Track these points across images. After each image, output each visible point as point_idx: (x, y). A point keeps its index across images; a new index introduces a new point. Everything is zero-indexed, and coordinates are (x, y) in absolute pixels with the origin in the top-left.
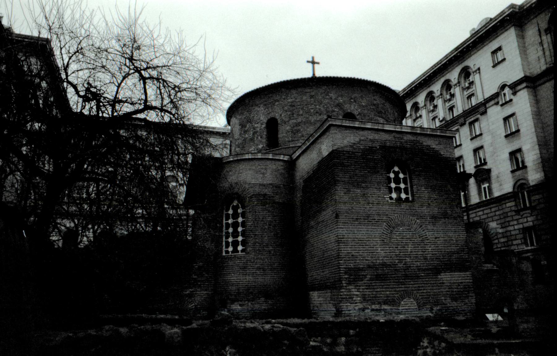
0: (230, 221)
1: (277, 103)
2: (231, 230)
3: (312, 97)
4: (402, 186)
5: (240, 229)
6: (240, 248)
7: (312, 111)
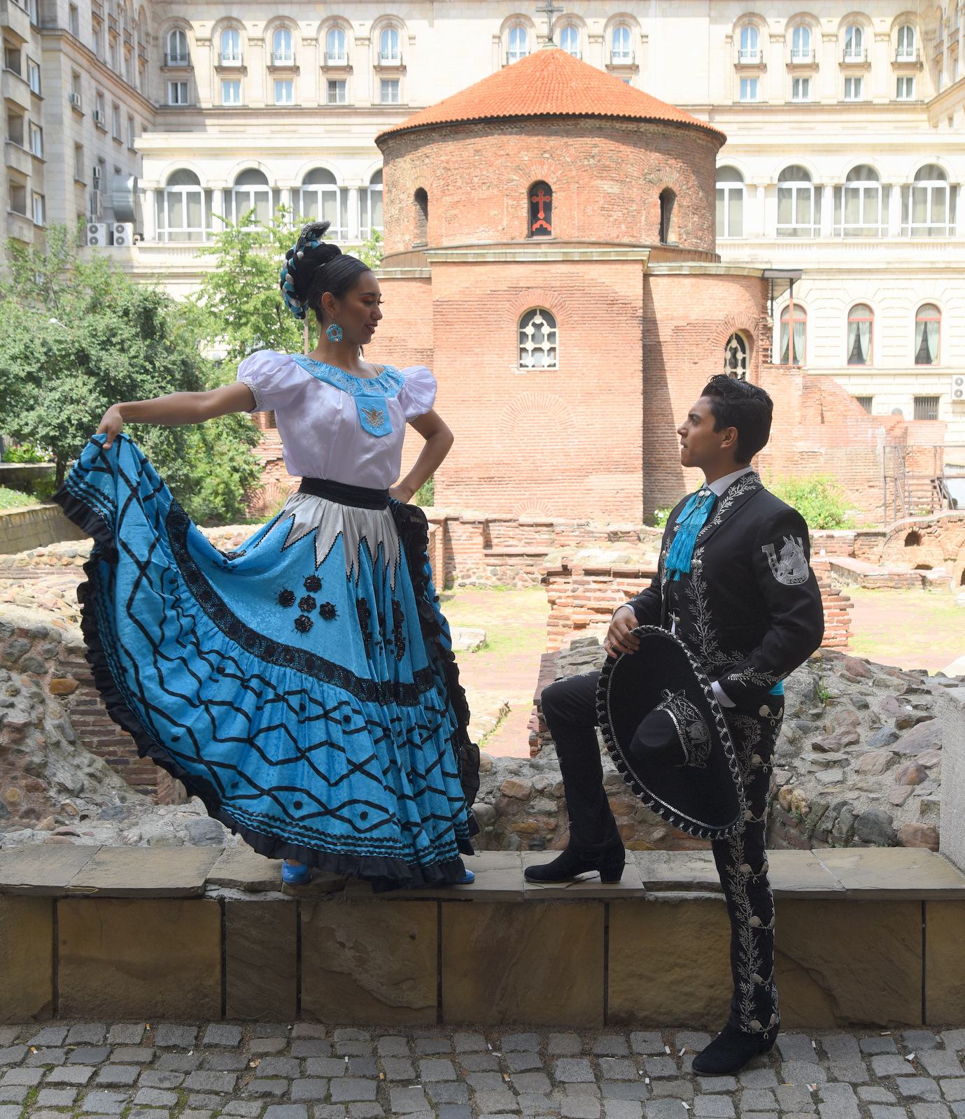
1: (427, 161)
7: (476, 180)
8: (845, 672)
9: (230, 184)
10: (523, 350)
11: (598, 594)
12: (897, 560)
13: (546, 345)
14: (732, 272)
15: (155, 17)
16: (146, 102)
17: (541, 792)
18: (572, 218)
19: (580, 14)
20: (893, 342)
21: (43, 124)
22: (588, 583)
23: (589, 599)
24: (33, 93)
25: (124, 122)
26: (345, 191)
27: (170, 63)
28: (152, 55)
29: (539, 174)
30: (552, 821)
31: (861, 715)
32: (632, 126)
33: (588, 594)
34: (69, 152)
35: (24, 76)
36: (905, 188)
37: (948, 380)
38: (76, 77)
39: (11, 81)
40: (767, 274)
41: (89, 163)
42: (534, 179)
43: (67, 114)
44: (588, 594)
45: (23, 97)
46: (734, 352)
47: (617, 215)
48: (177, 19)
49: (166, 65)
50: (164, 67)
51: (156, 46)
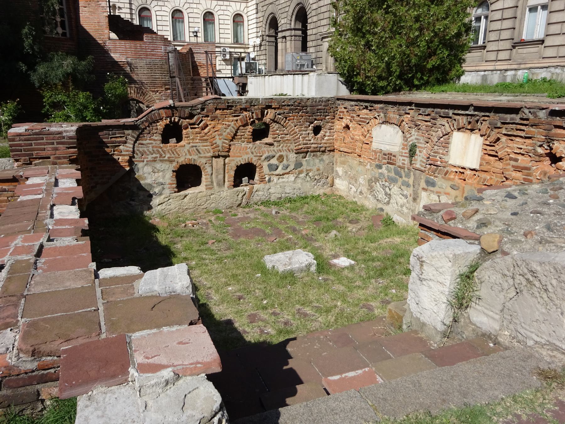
12: (154, 160)
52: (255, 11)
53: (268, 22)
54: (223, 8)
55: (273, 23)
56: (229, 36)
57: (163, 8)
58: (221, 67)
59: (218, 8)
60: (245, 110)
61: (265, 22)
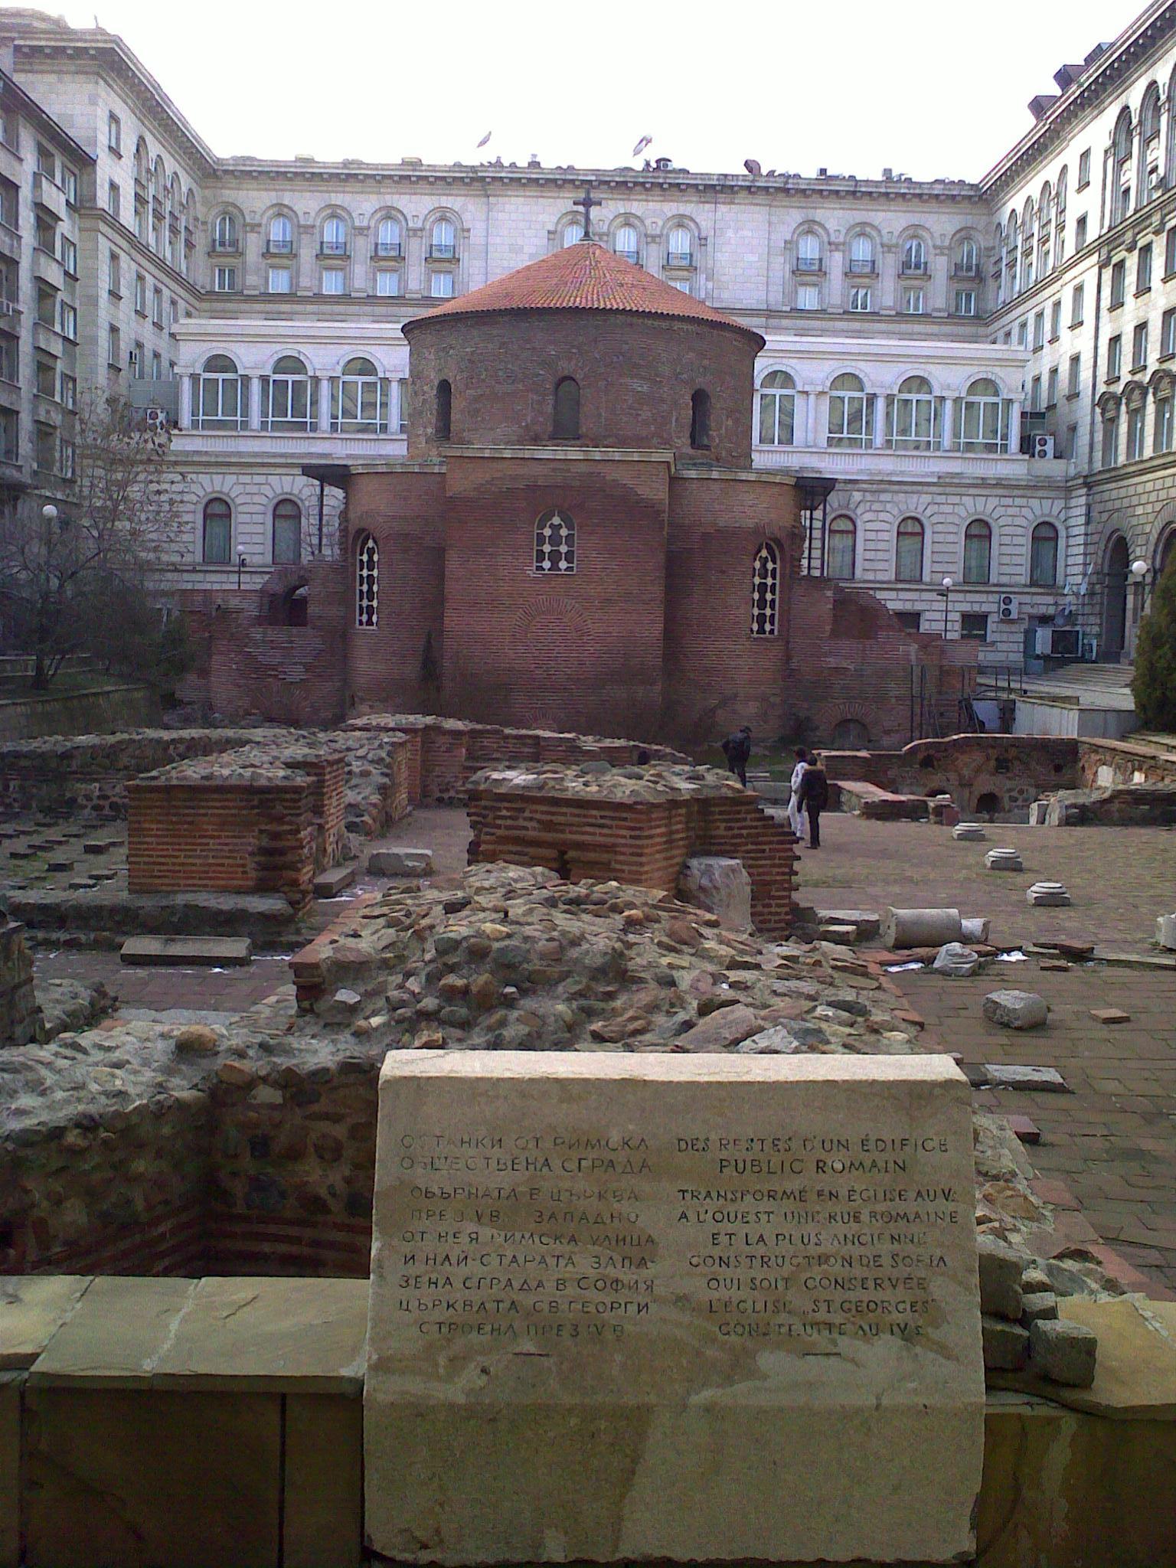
0: (365, 573)
2: (365, 588)
3: (503, 345)
4: (563, 549)
5: (375, 588)
6: (374, 618)
7: (500, 373)
8: (665, 939)
9: (268, 371)
10: (541, 553)
11: (509, 822)
12: (911, 784)
13: (563, 549)
14: (764, 478)
15: (205, 201)
16: (191, 289)
17: (264, 1080)
18: (600, 415)
19: (639, 214)
20: (945, 556)
21: (77, 306)
22: (499, 809)
23: (499, 827)
24: (66, 273)
25: (166, 305)
26: (386, 381)
27: (219, 249)
28: (201, 241)
29: (565, 367)
30: (277, 1115)
31: (665, 993)
32: (664, 325)
33: (499, 822)
34: (103, 335)
35: (58, 256)
36: (957, 400)
37: (997, 596)
38: (114, 257)
39: (43, 259)
40: (801, 482)
41: (125, 346)
42: (560, 374)
43: (104, 295)
44: (499, 822)
45: (54, 275)
46: (764, 561)
47: (646, 414)
48: (228, 204)
49: (214, 251)
50: (211, 253)
51: (205, 231)
52: (1082, 520)
53: (1110, 545)
54: (1011, 511)
55: (1120, 550)
56: (1021, 570)
57: (883, 516)
58: (996, 637)
59: (1001, 511)
60: (993, 747)
61: (1102, 546)
